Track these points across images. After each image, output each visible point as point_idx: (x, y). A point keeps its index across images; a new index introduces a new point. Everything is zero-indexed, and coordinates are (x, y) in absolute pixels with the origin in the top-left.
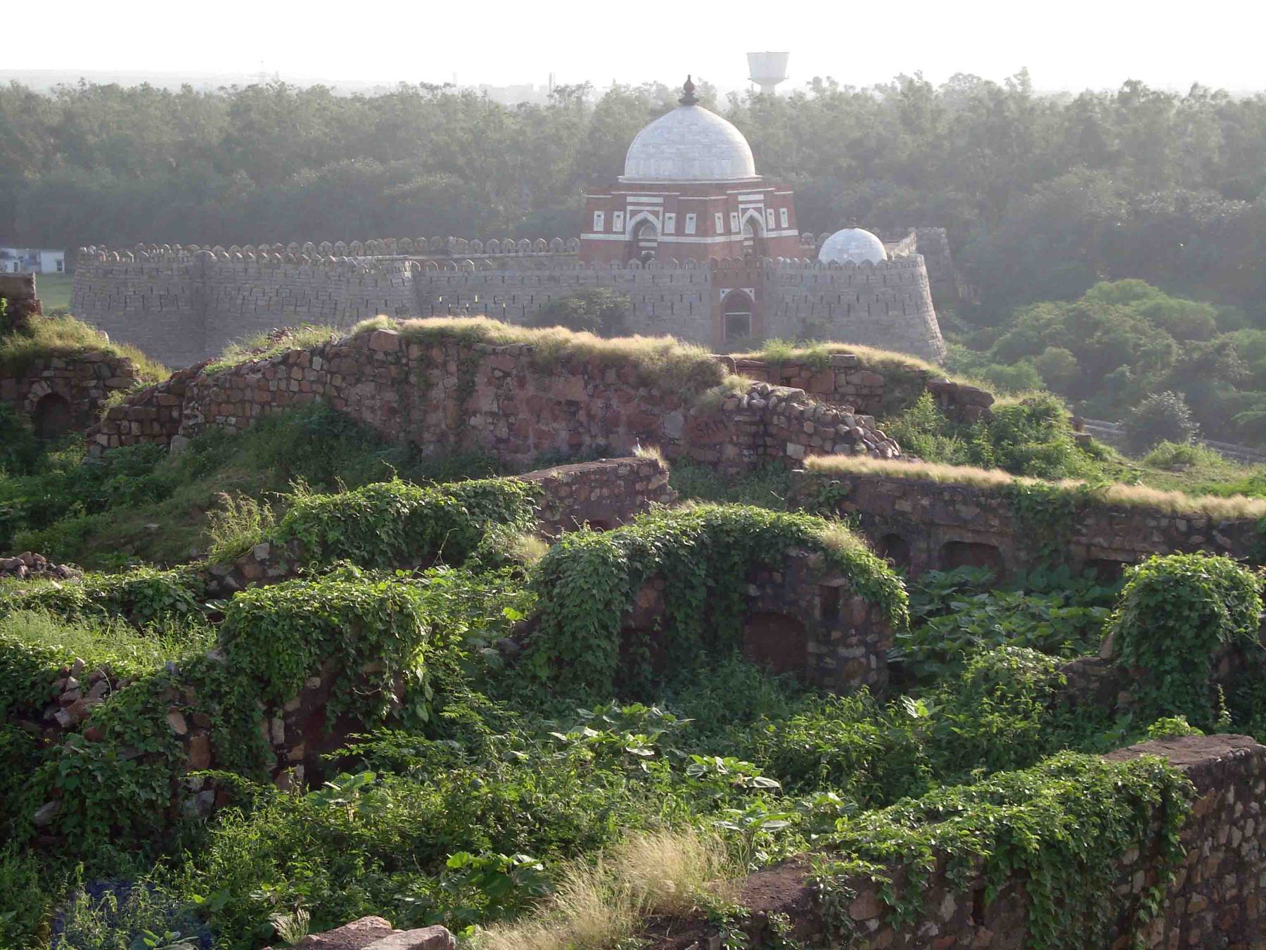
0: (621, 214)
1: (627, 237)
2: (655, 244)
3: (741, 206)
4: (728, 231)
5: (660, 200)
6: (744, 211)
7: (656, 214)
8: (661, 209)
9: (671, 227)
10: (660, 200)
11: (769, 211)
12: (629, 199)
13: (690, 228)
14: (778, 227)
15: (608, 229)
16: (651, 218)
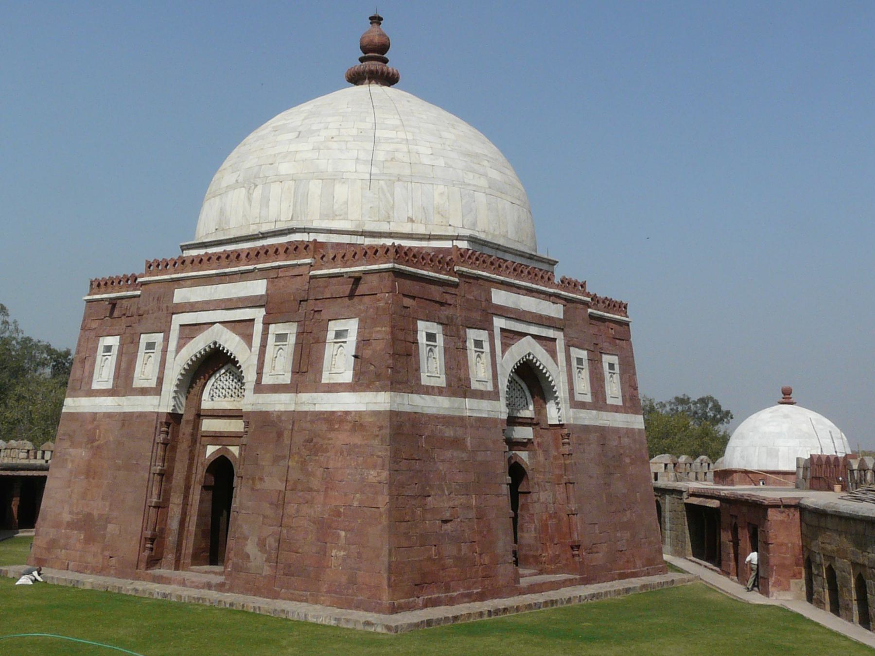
0: (158, 338)
1: (164, 403)
2: (236, 426)
3: (499, 323)
4: (458, 385)
5: (258, 287)
6: (511, 336)
7: (243, 327)
8: (258, 314)
9: (280, 365)
10: (258, 287)
11: (576, 353)
12: (181, 295)
13: (339, 361)
14: (599, 402)
15: (123, 383)
16: (231, 343)
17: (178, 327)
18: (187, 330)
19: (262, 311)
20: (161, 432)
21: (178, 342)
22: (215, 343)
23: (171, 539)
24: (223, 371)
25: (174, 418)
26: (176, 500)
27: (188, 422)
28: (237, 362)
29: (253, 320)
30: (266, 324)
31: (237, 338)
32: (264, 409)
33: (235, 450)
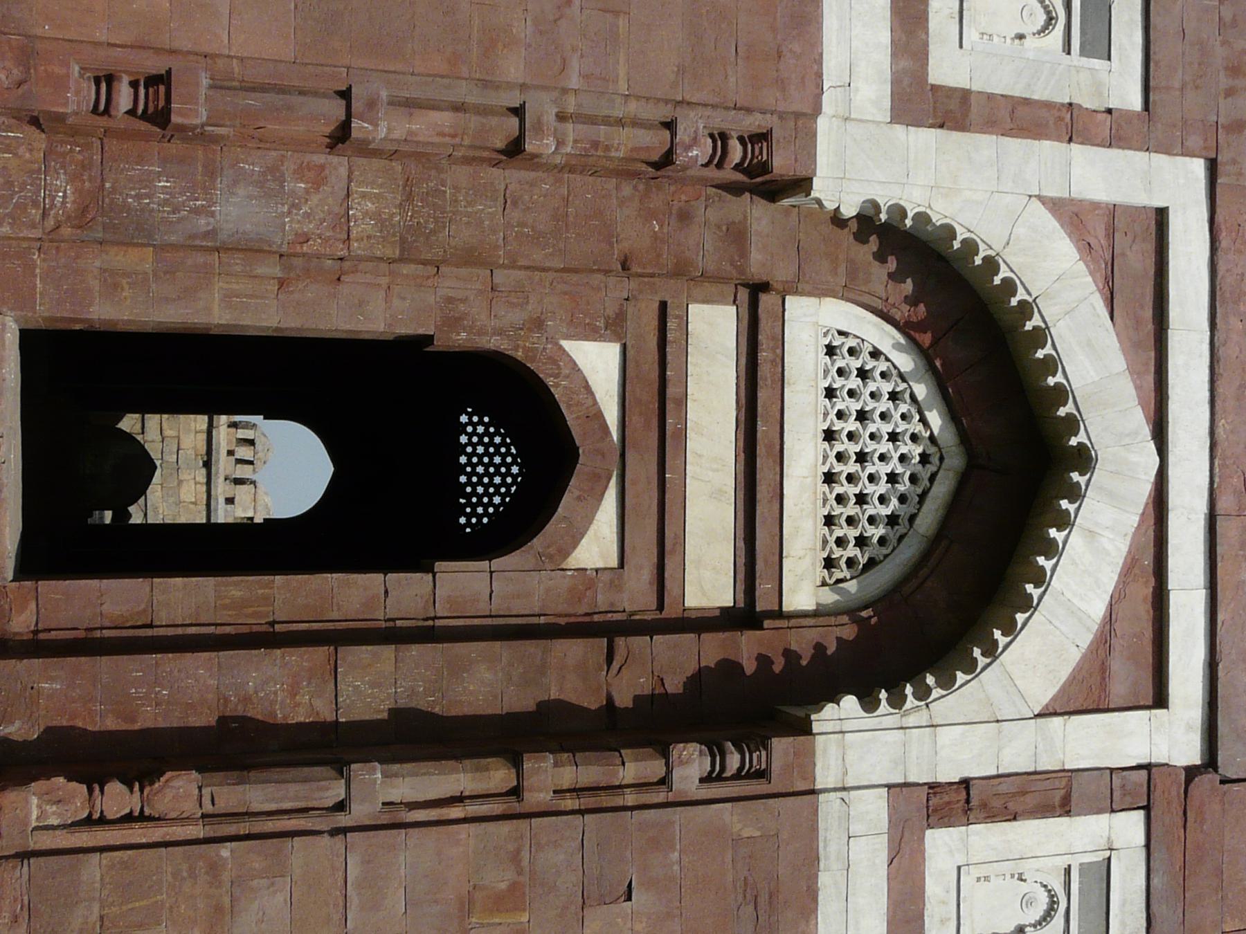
17: (1161, 204)
18: (1138, 259)
19: (1188, 752)
20: (721, 138)
21: (1095, 205)
22: (1084, 459)
23: (152, 182)
24: (936, 419)
25: (767, 175)
26: (371, 199)
27: (737, 236)
28: (1010, 629)
29: (1160, 700)
30: (1140, 788)
31: (1097, 609)
32: (824, 879)
33: (597, 546)
